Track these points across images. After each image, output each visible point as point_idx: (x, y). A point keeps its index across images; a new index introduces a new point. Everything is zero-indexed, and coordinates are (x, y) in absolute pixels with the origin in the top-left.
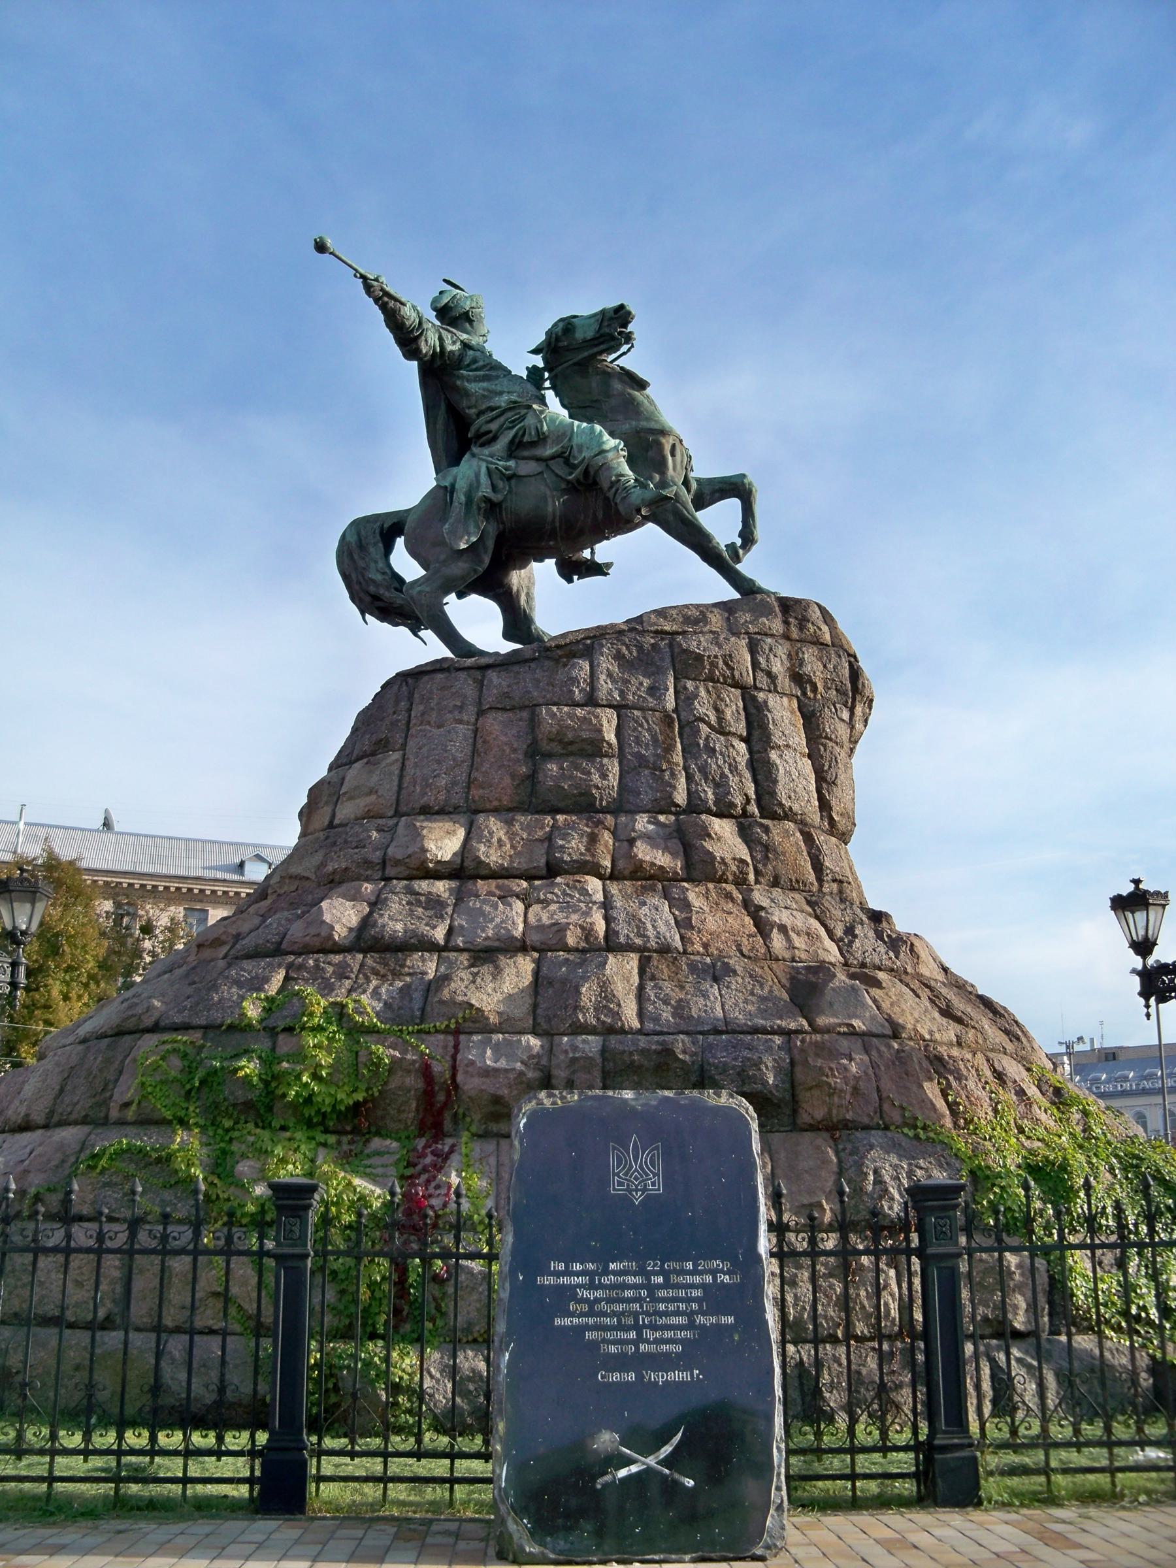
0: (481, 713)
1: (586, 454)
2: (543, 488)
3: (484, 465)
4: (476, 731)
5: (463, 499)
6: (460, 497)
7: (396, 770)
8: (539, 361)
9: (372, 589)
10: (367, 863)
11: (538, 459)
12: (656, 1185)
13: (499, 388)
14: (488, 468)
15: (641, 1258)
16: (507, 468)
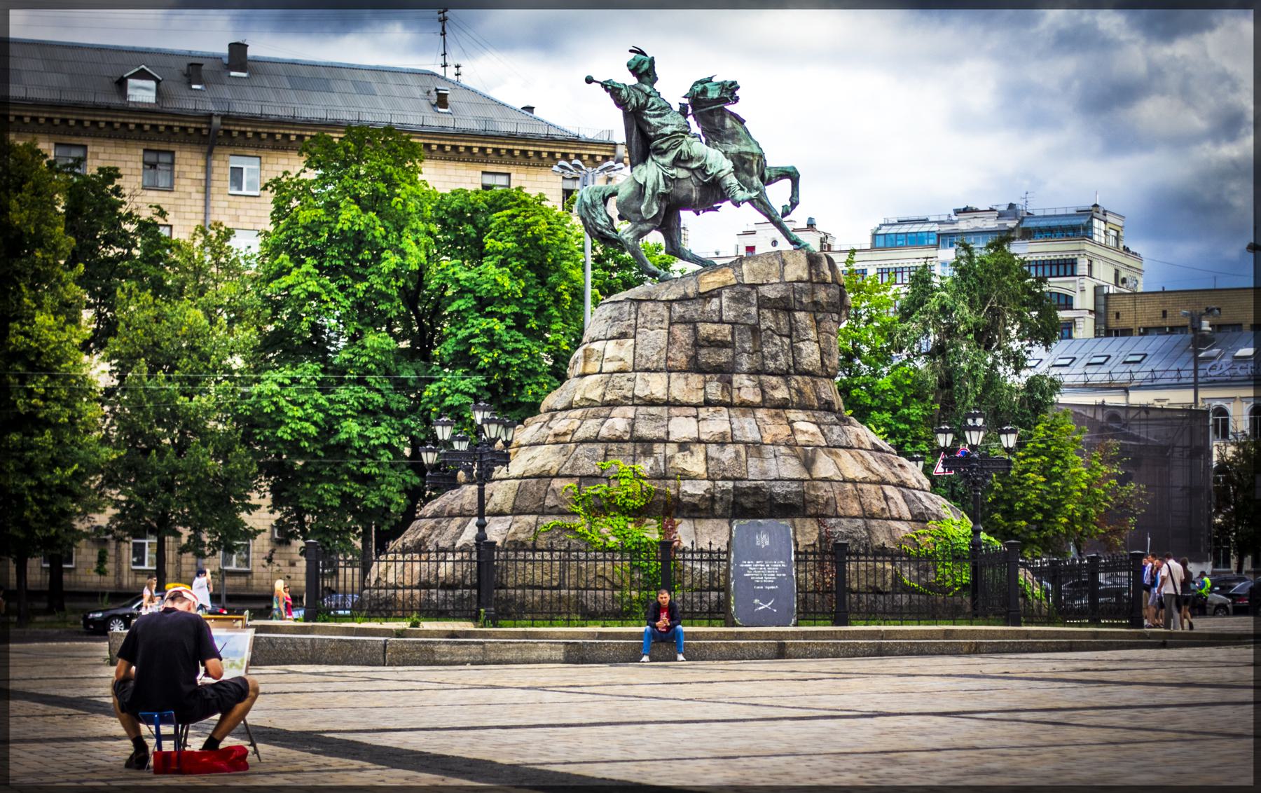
0: (671, 324)
1: (711, 171)
2: (691, 185)
3: (661, 172)
4: (669, 333)
5: (650, 192)
6: (649, 192)
7: (631, 349)
8: (686, 101)
9: (599, 228)
10: (626, 398)
11: (688, 169)
12: (767, 543)
13: (666, 122)
14: (663, 175)
15: (764, 560)
16: (673, 175)
